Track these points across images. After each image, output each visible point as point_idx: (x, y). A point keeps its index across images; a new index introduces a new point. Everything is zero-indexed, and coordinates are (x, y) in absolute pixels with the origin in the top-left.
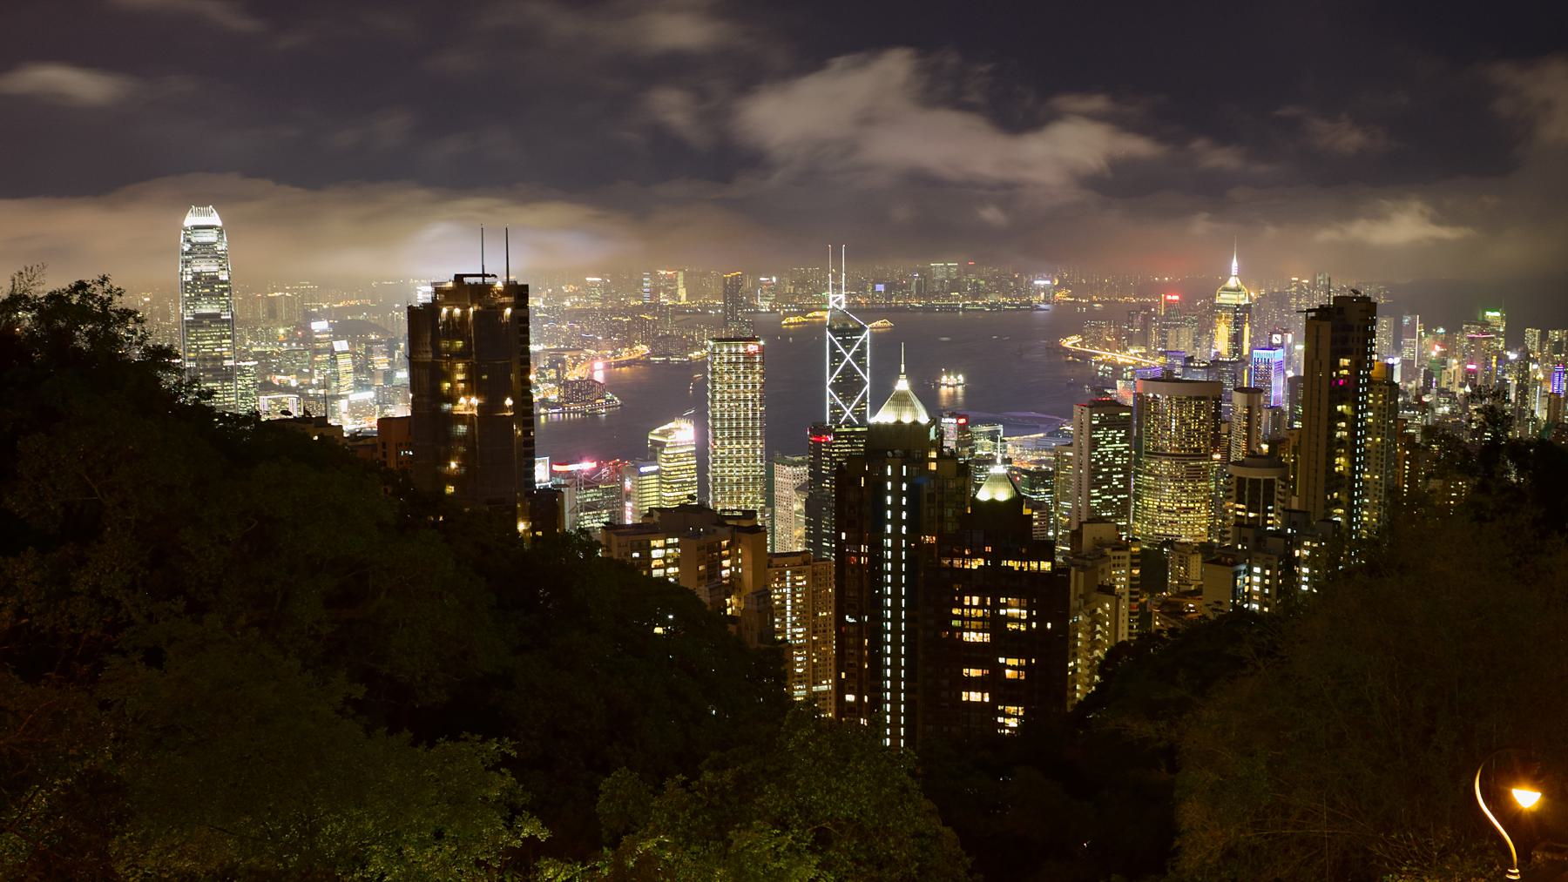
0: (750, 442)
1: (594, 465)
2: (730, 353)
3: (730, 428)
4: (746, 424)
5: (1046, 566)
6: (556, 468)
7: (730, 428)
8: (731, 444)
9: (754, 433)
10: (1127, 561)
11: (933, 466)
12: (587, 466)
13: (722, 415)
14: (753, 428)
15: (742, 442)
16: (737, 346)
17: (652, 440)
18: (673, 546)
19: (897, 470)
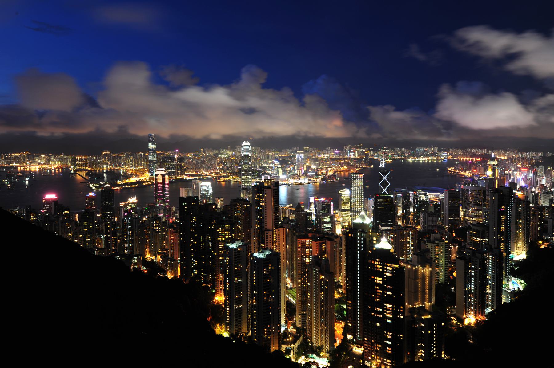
0: (360, 196)
1: (324, 199)
2: (355, 177)
3: (356, 193)
4: (359, 192)
5: (397, 266)
6: (316, 199)
7: (356, 193)
8: (356, 196)
9: (361, 194)
10: (444, 244)
11: (371, 234)
12: (322, 199)
13: (354, 190)
14: (361, 193)
15: (358, 196)
16: (356, 175)
17: (340, 193)
18: (311, 242)
19: (360, 234)
